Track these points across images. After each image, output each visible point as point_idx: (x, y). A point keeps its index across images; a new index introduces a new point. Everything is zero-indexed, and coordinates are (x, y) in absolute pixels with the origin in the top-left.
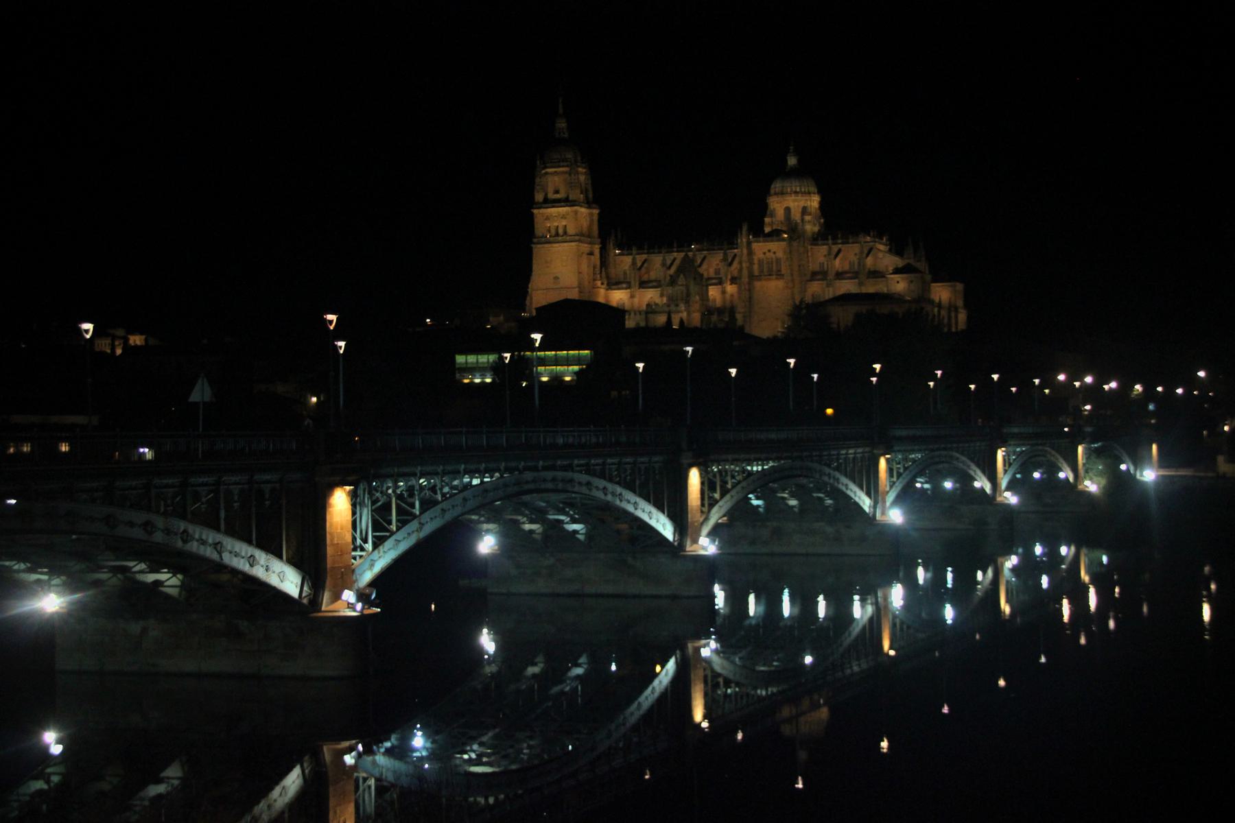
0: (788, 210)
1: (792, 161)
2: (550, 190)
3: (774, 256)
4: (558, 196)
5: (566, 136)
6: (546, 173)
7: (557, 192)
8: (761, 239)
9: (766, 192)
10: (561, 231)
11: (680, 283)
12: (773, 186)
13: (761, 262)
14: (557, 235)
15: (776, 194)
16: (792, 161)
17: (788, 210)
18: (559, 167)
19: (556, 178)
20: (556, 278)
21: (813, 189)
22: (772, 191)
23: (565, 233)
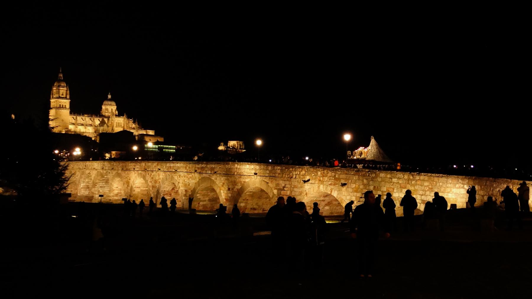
0: (112, 109)
1: (109, 97)
2: (61, 93)
3: (120, 122)
4: (63, 96)
5: (62, 79)
6: (59, 89)
7: (62, 95)
8: (117, 117)
9: (102, 104)
10: (64, 106)
11: (105, 126)
12: (104, 103)
13: (117, 123)
14: (63, 107)
15: (105, 105)
16: (109, 97)
17: (112, 109)
18: (64, 88)
19: (63, 91)
20: (62, 120)
21: (115, 104)
22: (104, 104)
23: (65, 108)
